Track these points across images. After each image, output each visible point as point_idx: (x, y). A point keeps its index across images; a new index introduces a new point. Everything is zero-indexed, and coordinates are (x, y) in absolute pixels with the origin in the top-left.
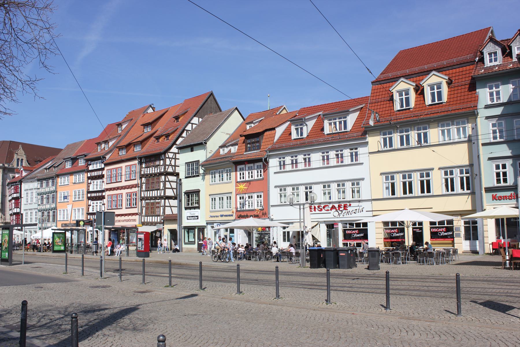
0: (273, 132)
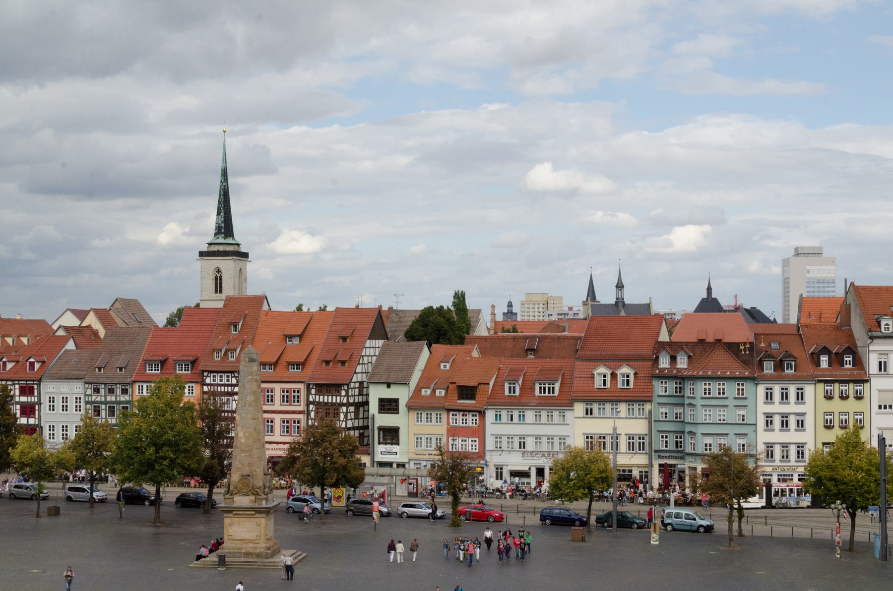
0: (486, 386)
